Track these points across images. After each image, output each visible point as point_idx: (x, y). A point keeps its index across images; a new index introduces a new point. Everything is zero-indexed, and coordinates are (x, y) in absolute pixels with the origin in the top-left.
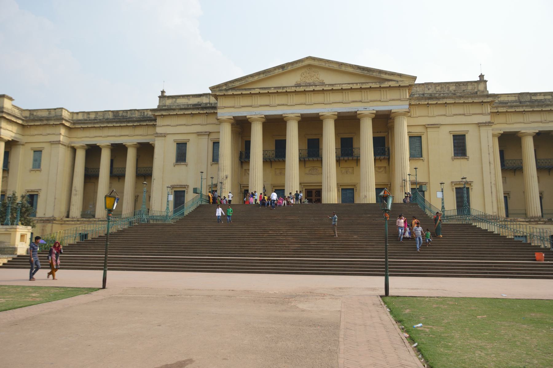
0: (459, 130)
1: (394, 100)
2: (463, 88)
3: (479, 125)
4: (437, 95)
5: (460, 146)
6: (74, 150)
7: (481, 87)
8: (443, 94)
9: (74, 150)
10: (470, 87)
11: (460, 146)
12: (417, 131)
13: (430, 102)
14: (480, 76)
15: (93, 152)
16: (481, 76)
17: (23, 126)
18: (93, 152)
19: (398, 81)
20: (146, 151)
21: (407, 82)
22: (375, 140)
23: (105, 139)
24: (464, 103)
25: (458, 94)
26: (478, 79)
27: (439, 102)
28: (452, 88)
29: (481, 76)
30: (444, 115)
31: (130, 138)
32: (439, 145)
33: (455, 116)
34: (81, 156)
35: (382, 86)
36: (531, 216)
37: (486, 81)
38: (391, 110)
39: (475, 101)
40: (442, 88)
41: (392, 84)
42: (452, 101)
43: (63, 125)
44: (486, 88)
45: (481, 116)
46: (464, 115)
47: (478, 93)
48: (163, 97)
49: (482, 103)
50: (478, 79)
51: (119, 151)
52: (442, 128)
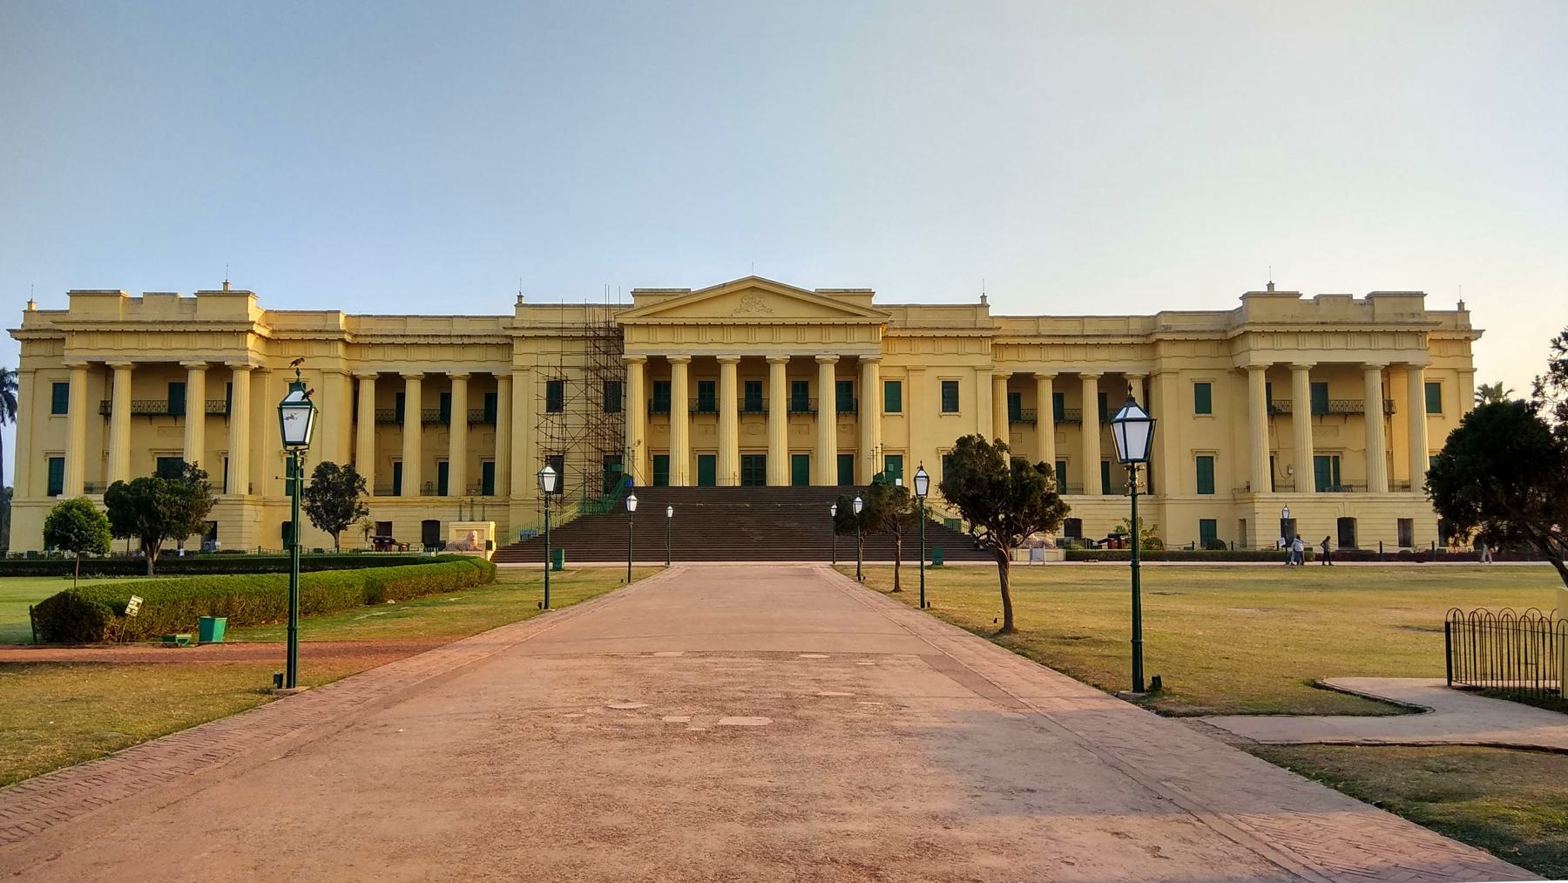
0: (950, 375)
3: (975, 369)
5: (950, 397)
6: (356, 382)
9: (356, 382)
11: (950, 397)
12: (894, 375)
15: (390, 385)
16: (984, 297)
17: (267, 340)
18: (390, 385)
20: (485, 387)
22: (838, 384)
23: (412, 366)
29: (984, 297)
31: (458, 366)
32: (923, 396)
34: (368, 391)
43: (343, 340)
48: (519, 305)
51: (437, 385)
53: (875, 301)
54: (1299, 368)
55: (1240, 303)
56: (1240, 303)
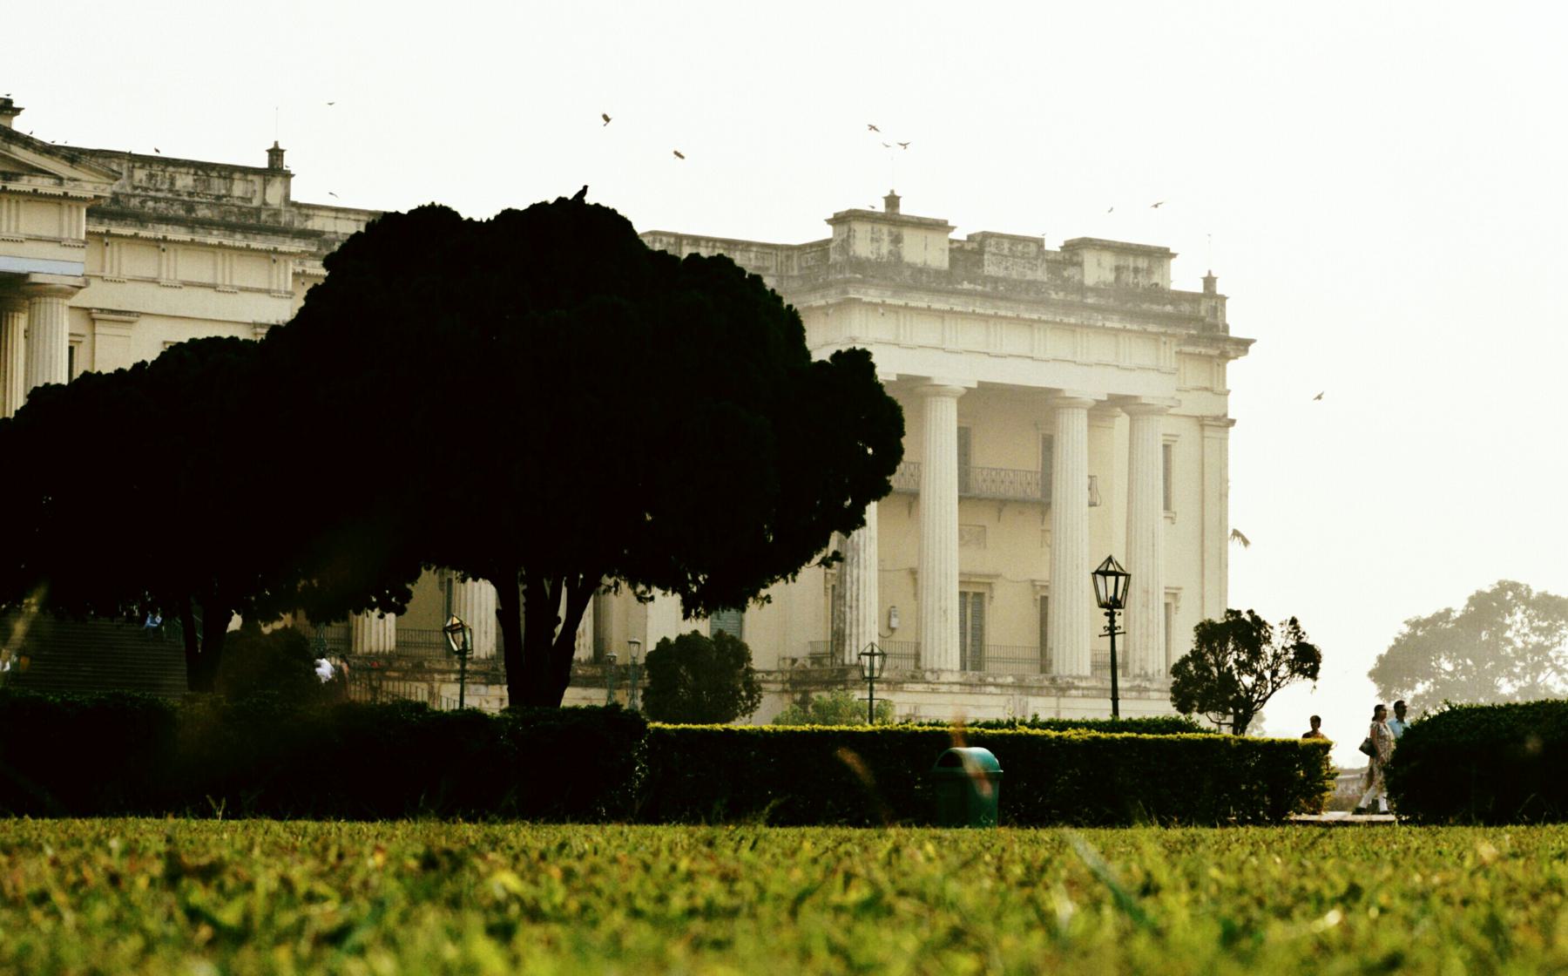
1: (39, 239)
2: (218, 186)
4: (135, 202)
7: (274, 195)
8: (156, 200)
10: (239, 188)
13: (115, 230)
14: (270, 151)
16: (276, 153)
19: (60, 179)
21: (89, 187)
24: (221, 246)
25: (203, 212)
26: (263, 162)
27: (143, 233)
28: (185, 181)
29: (276, 153)
30: (154, 281)
33: (185, 289)
35: (12, 186)
36: (366, 649)
37: (288, 176)
38: (26, 276)
39: (254, 245)
40: (151, 176)
41: (44, 185)
42: (181, 234)
44: (287, 196)
45: (264, 297)
46: (214, 287)
47: (263, 217)
49: (272, 255)
50: (263, 162)
52: (144, 323)
53: (19, 125)
54: (940, 391)
55: (827, 232)
56: (827, 232)
